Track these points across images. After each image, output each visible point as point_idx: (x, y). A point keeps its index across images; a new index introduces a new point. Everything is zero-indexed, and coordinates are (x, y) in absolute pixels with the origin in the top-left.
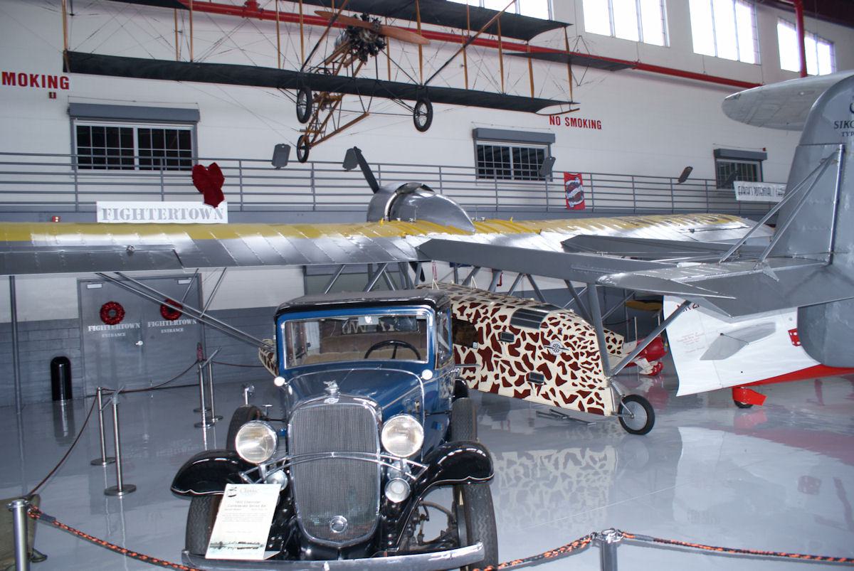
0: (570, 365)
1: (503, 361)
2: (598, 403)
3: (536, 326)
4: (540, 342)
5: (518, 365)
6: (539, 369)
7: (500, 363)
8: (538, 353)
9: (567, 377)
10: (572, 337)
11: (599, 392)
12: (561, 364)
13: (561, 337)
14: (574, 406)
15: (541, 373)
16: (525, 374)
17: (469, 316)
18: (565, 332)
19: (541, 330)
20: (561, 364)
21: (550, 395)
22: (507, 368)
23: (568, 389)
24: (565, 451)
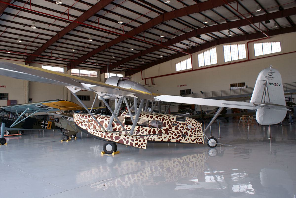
0: (194, 131)
1: (172, 132)
2: (201, 141)
3: (184, 121)
5: (178, 133)
6: (184, 133)
7: (172, 132)
8: (185, 128)
9: (193, 135)
10: (194, 124)
11: (202, 138)
12: (191, 131)
13: (191, 124)
14: (195, 142)
15: (185, 134)
16: (180, 135)
18: (192, 122)
19: (186, 122)
20: (191, 131)
21: (188, 140)
22: (174, 134)
23: (193, 138)
24: (192, 156)
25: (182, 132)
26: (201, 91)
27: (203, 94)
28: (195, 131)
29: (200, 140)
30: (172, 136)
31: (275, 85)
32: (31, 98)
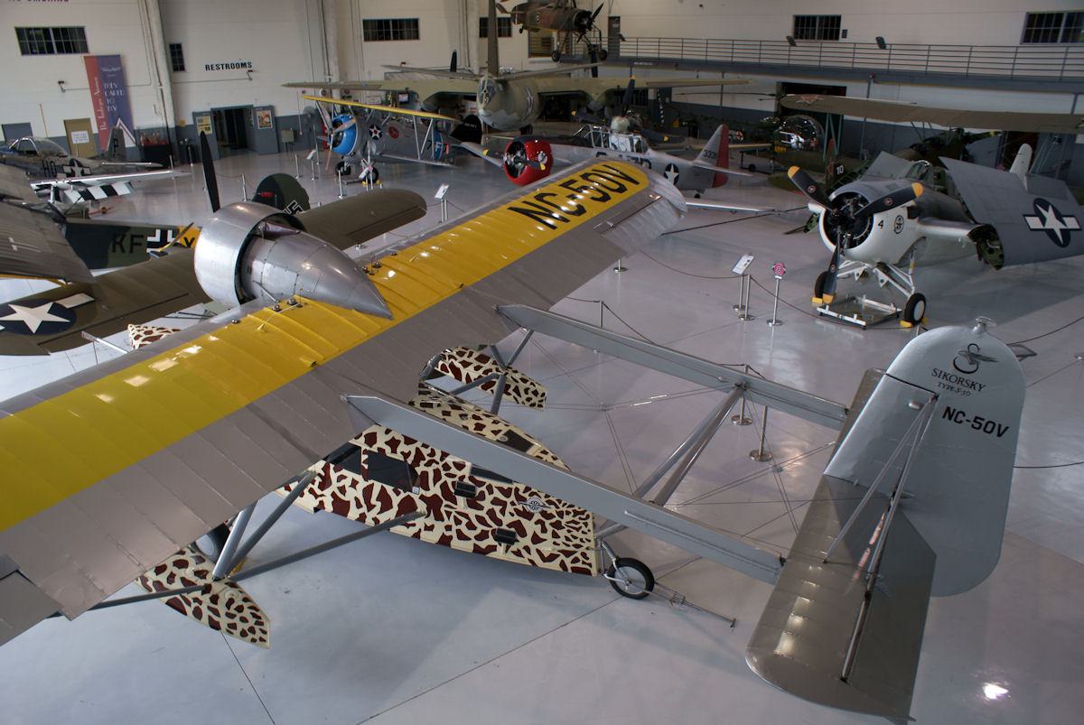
0: (551, 524)
2: (584, 563)
4: (513, 498)
6: (509, 525)
8: (510, 508)
9: (548, 536)
11: (586, 552)
14: (555, 565)
15: (513, 529)
16: (490, 529)
17: (406, 455)
22: (465, 521)
23: (547, 548)
25: (499, 522)
26: (877, 38)
27: (887, 52)
28: (557, 525)
29: (581, 558)
30: (455, 528)
31: (977, 425)
32: (176, 41)
